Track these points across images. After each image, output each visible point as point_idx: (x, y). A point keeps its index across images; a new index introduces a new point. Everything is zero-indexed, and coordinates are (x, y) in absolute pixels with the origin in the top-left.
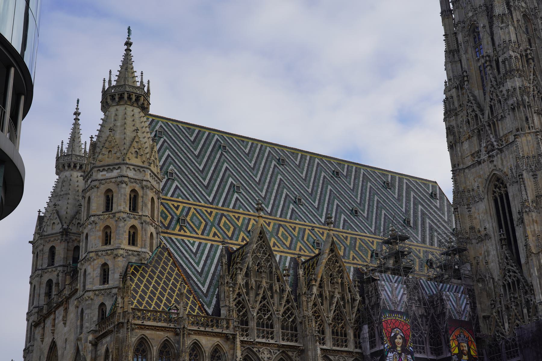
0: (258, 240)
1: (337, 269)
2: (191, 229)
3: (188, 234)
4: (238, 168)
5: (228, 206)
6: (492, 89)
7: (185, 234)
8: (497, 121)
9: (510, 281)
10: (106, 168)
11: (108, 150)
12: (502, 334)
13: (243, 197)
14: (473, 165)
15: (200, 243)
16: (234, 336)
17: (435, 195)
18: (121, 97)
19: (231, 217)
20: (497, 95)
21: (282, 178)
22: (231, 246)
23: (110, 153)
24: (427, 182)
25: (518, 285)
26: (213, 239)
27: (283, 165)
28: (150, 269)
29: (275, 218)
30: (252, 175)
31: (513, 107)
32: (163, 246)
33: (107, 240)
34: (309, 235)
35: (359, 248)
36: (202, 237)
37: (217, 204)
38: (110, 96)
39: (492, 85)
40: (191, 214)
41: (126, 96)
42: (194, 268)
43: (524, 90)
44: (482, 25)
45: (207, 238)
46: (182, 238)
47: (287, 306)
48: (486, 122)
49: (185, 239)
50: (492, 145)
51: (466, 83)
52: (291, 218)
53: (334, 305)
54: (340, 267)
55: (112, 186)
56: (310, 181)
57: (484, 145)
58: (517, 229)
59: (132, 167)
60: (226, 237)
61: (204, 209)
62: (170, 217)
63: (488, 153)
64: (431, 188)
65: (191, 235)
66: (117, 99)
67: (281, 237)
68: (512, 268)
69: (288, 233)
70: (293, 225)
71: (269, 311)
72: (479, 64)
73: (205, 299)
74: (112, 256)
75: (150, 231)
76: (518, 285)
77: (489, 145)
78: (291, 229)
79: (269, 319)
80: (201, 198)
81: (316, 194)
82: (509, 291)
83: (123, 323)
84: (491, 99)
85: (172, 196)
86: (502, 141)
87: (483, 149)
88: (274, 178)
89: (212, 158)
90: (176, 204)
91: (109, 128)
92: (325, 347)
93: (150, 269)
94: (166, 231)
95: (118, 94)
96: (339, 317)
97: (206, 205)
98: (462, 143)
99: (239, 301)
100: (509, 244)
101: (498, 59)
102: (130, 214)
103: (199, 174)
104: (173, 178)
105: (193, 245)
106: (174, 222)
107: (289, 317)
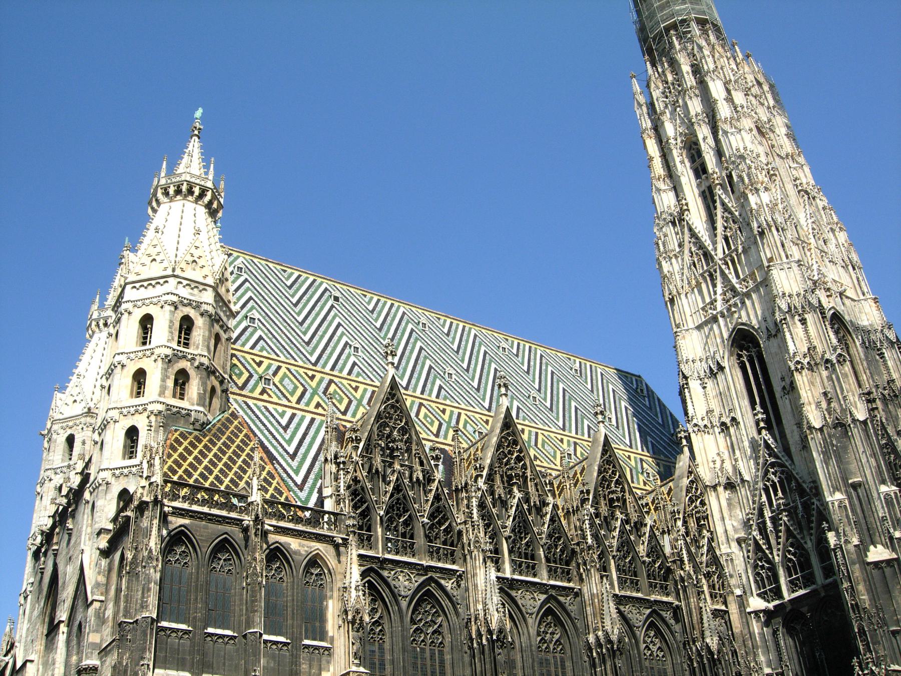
0: (388, 399)
1: (515, 455)
2: (279, 394)
3: (275, 400)
4: (357, 327)
5: (341, 371)
6: (726, 214)
7: (270, 399)
8: (737, 255)
9: (776, 481)
10: (145, 284)
11: (151, 258)
12: (769, 561)
13: (363, 362)
14: (706, 323)
15: (293, 415)
16: (345, 541)
17: (642, 390)
18: (178, 192)
19: (344, 386)
20: (734, 222)
21: (423, 346)
22: (344, 423)
23: (154, 262)
24: (629, 376)
25: (789, 484)
26: (316, 411)
27: (424, 330)
28: (207, 438)
29: (414, 394)
30: (378, 337)
31: (760, 230)
32: (233, 412)
33: (139, 393)
34: (466, 422)
35: (543, 446)
36: (297, 406)
37: (324, 367)
38: (161, 189)
39: (724, 209)
40: (280, 374)
41: (184, 188)
42: (283, 447)
43: (773, 207)
44: (702, 137)
45: (306, 408)
46: (265, 404)
47: (436, 505)
48: (720, 259)
49: (270, 406)
50: (733, 289)
51: (686, 213)
52: (438, 396)
53: (514, 509)
54: (520, 451)
55: (152, 310)
56: (464, 353)
57: (719, 290)
58: (780, 403)
59: (185, 282)
60: (337, 411)
61: (301, 371)
62: (246, 375)
63: (728, 301)
64: (634, 382)
65: (280, 402)
66: (171, 191)
67: (423, 420)
68: (779, 461)
69: (435, 417)
70: (442, 407)
71: (407, 511)
72: (702, 189)
73: (300, 494)
74: (146, 414)
75: (212, 383)
76: (789, 484)
77: (727, 291)
78: (439, 412)
79: (406, 523)
80: (299, 357)
81: (475, 371)
82: (776, 495)
83: (147, 503)
84: (726, 228)
85: (253, 347)
86: (748, 282)
87: (719, 298)
88: (410, 346)
89: (317, 309)
90: (258, 359)
91: (154, 228)
92: (500, 574)
93: (207, 438)
94: (238, 391)
95: (174, 186)
96: (522, 527)
97: (305, 366)
98: (686, 295)
99: (356, 490)
100: (769, 428)
101: (730, 173)
102: (178, 351)
103: (296, 326)
104: (256, 325)
105: (282, 415)
106: (252, 382)
107: (440, 523)
